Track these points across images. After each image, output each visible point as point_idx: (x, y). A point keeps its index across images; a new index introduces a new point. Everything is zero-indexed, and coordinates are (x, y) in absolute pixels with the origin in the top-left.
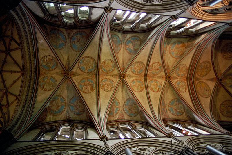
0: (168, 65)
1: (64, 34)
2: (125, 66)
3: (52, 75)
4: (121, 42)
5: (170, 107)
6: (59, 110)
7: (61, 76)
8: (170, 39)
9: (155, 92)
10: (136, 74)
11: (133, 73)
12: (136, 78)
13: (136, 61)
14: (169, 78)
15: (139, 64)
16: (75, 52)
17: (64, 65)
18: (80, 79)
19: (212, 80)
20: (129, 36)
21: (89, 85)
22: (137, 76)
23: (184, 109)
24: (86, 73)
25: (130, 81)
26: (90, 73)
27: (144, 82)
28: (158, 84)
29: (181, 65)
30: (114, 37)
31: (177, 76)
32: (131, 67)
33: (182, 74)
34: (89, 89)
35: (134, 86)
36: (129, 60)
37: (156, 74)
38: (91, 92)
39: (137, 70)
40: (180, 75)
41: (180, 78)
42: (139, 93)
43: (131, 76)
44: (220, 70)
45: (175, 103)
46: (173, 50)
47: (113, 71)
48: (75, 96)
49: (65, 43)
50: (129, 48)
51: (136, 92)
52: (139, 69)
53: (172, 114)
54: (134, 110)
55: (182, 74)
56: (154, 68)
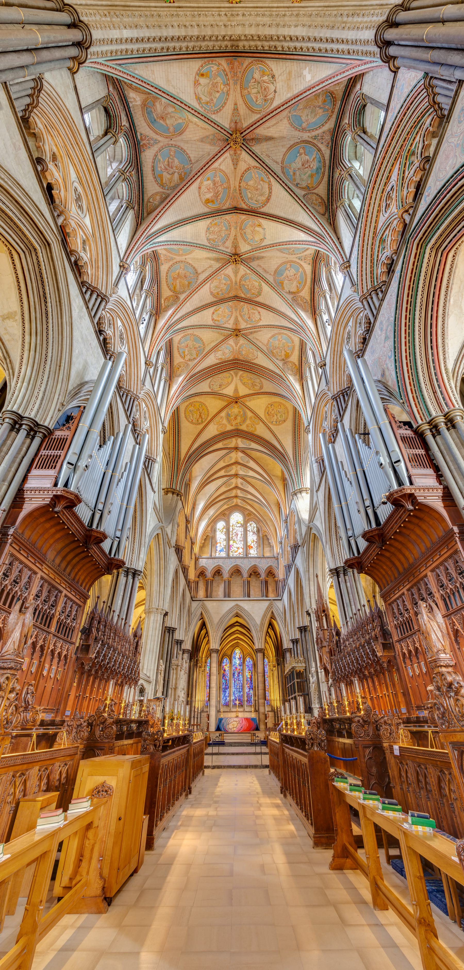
1: (323, 125)
2: (254, 264)
3: (231, 96)
6: (155, 120)
7: (231, 121)
13: (263, 284)
14: (237, 335)
16: (282, 157)
17: (255, 131)
18: (226, 171)
19: (236, 390)
20: (308, 269)
21: (216, 195)
23: (190, 360)
24: (240, 183)
26: (240, 194)
27: (227, 296)
34: (209, 196)
35: (220, 280)
36: (265, 271)
39: (248, 283)
43: (236, 273)
44: (250, 401)
45: (197, 345)
47: (245, 241)
48: (191, 161)
50: (286, 269)
54: (178, 284)
55: (244, 353)
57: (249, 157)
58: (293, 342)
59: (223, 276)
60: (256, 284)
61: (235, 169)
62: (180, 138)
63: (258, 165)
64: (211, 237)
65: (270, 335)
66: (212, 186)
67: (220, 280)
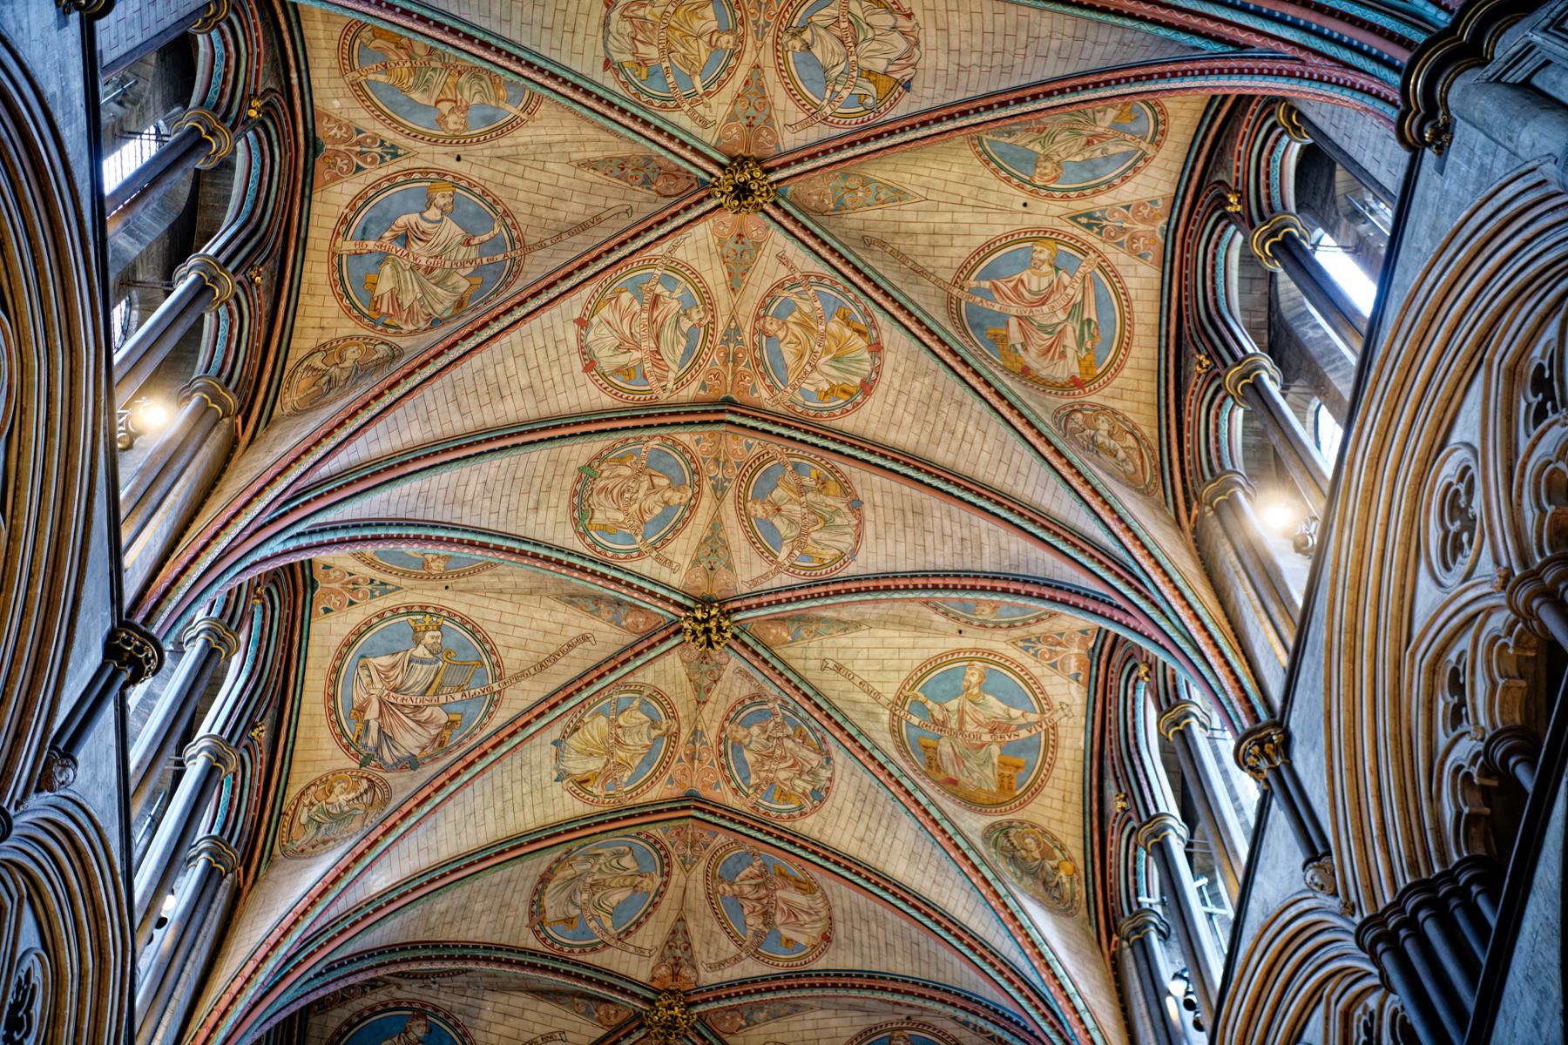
0: (610, 159)
4: (395, 611)
5: (1055, 179)
8: (325, 130)
9: (878, 370)
10: (697, 496)
11: (685, 522)
12: (730, 494)
13: (566, 537)
14: (742, 192)
15: (595, 499)
22: (715, 488)
24: (665, 884)
25: (756, 557)
26: (666, 856)
28: (807, 309)
29: (607, 64)
30: (359, 695)
31: (731, 72)
32: (629, 557)
33: (713, 25)
34: (798, 899)
35: (800, 540)
37: (696, 317)
38: (824, 894)
40: (726, 41)
41: (750, 41)
42: (869, 529)
43: (714, 542)
46: (445, 107)
47: (657, 694)
49: (421, 1013)
51: (854, 552)
52: (645, 485)
53: (1135, 169)
56: (638, 348)
57: (622, 970)
58: (357, 86)
59: (782, 556)
60: (606, 513)
61: (681, 920)
62: (876, 1020)
63: (590, 958)
64: (815, 759)
65: (523, 135)
66: (779, 919)
67: (800, 540)
